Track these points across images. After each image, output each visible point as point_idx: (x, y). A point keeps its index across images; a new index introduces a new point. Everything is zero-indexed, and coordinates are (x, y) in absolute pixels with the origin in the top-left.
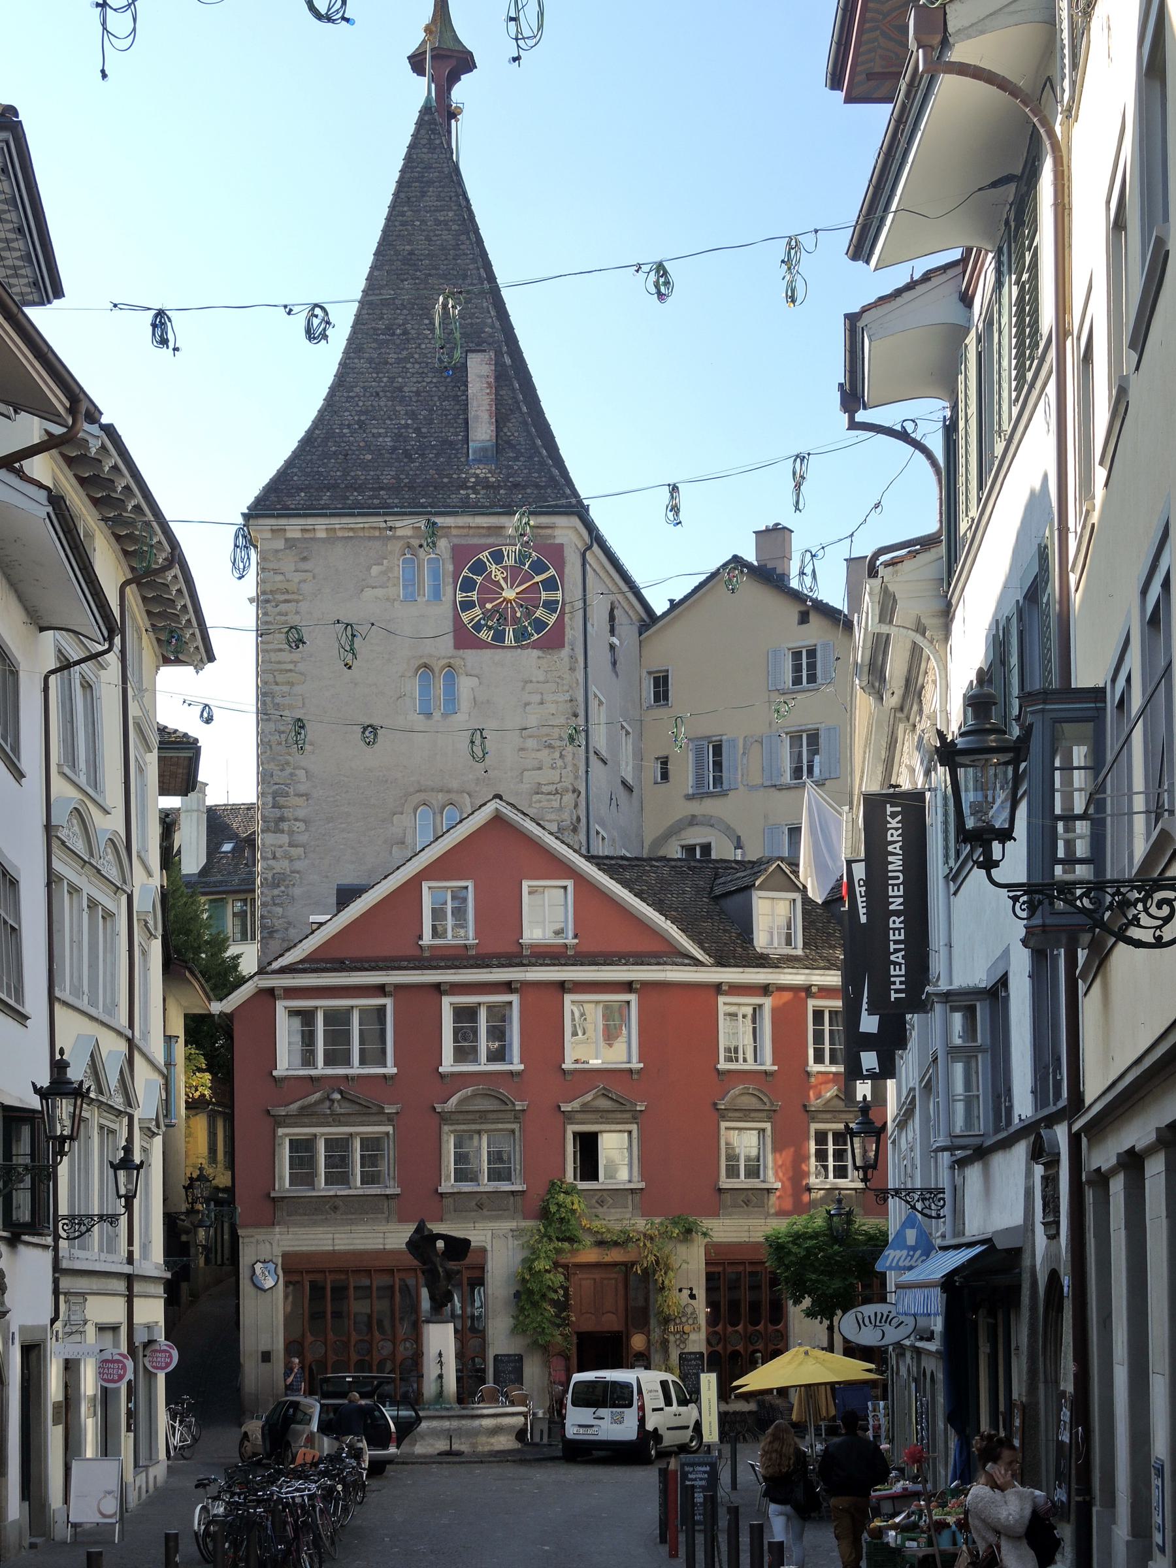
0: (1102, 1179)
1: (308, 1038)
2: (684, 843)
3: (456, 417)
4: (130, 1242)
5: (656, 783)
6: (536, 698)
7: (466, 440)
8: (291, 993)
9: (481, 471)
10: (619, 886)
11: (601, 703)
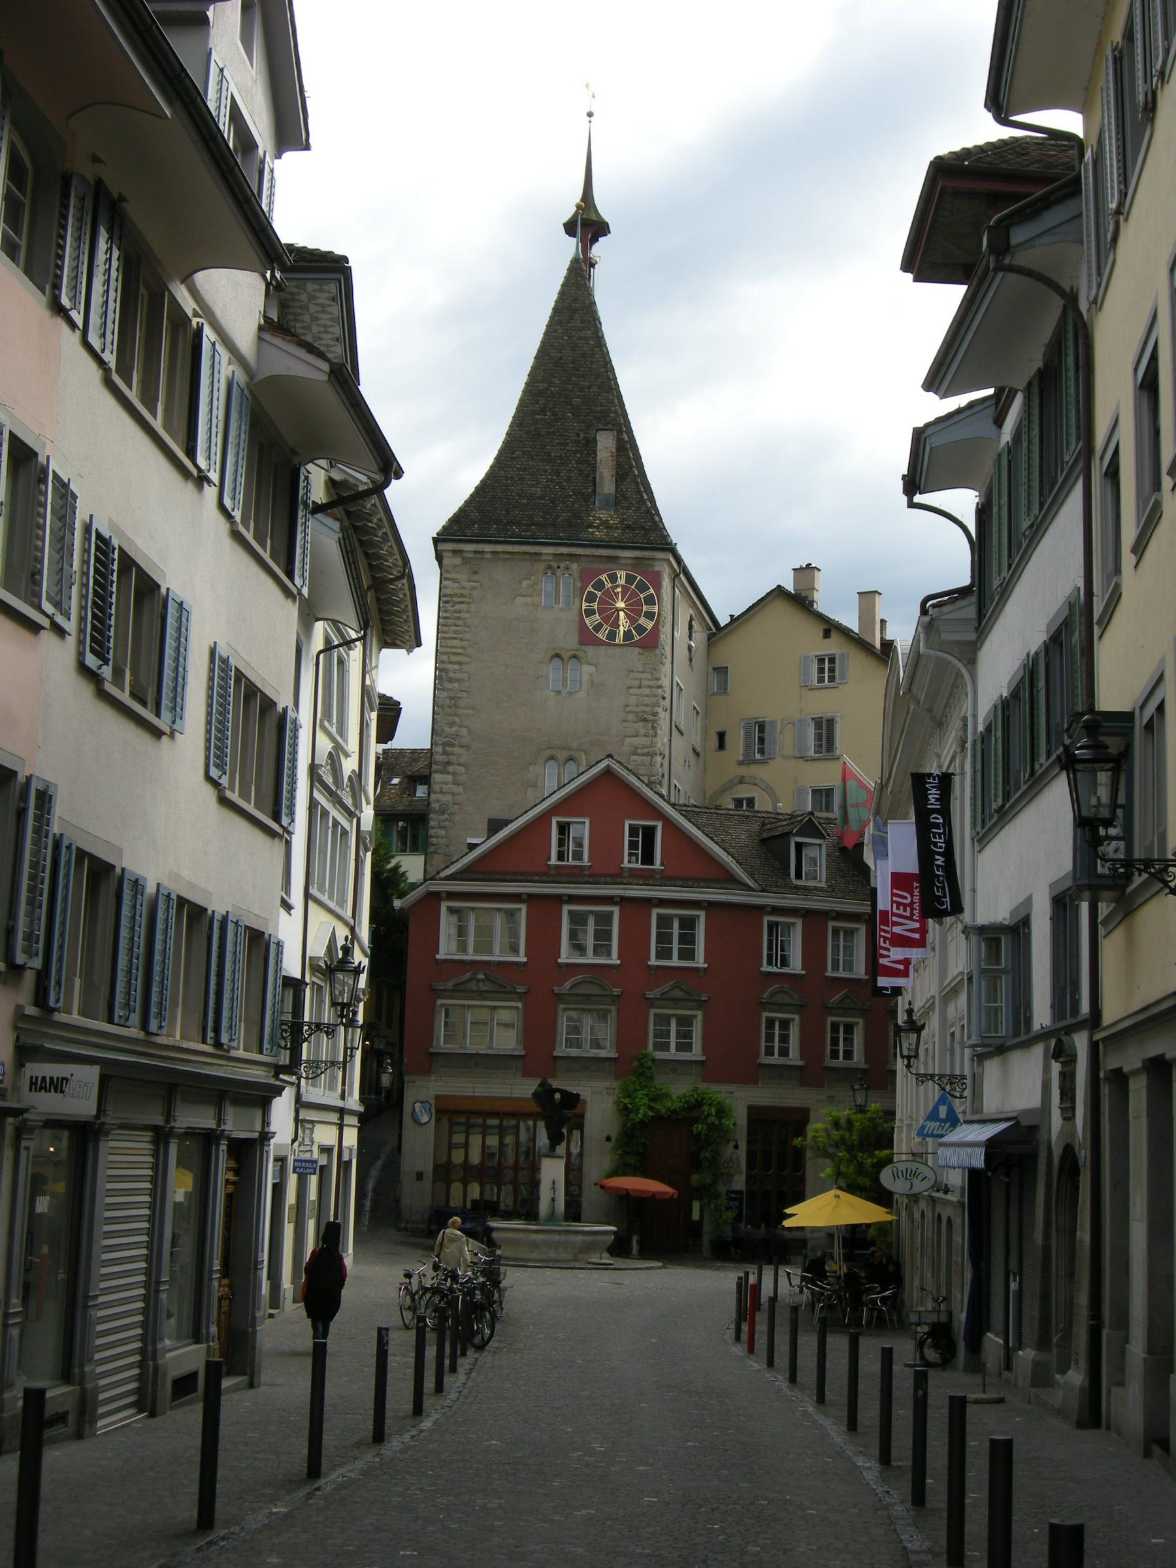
0: (1120, 1078)
3: (588, 475)
4: (344, 1084)
6: (636, 683)
7: (594, 491)
9: (603, 515)
11: (681, 689)
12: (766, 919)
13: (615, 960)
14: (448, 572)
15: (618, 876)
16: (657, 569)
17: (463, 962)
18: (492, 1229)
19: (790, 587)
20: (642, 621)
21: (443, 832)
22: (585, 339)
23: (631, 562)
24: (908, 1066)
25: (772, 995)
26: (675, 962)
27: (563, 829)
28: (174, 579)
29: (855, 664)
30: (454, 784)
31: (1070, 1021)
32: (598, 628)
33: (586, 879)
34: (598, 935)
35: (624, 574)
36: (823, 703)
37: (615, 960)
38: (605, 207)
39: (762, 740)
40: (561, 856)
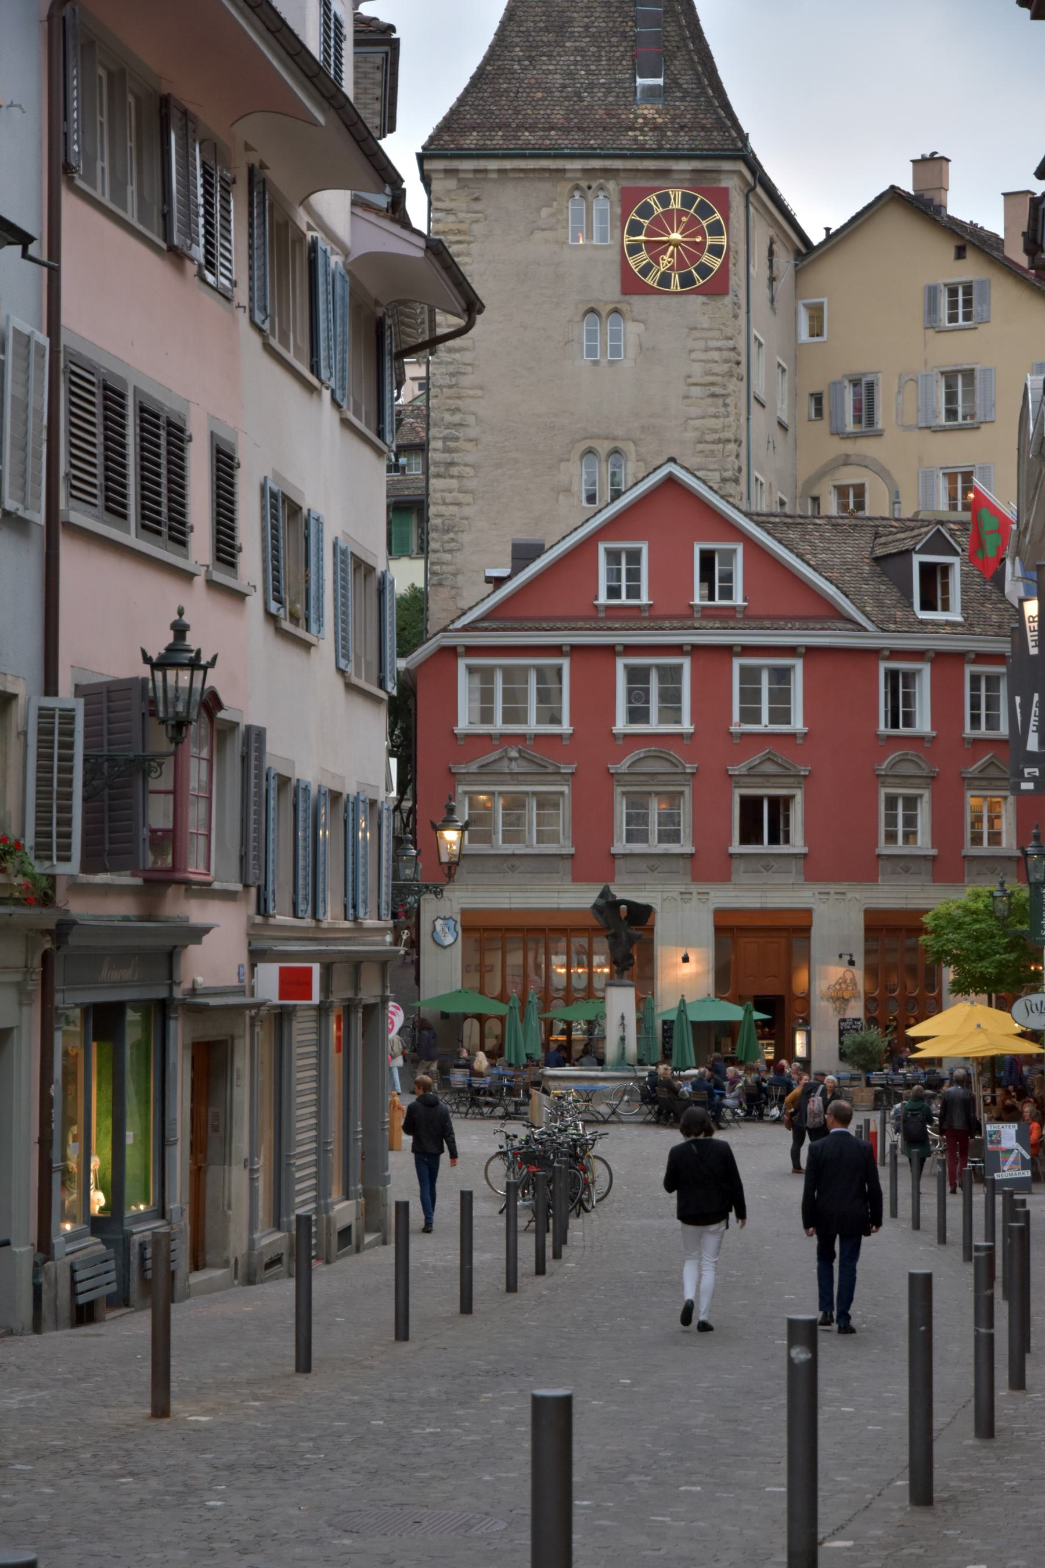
1: (487, 696)
2: (837, 483)
5: (810, 420)
6: (701, 344)
8: (472, 651)
10: (787, 551)
11: (760, 345)
12: (883, 666)
13: (686, 726)
14: (439, 200)
15: (687, 617)
16: (724, 184)
17: (489, 736)
19: (907, 186)
20: (706, 258)
21: (447, 557)
23: (688, 176)
25: (893, 765)
26: (765, 725)
27: (613, 556)
28: (310, 501)
30: (460, 491)
32: (646, 270)
33: (645, 624)
34: (663, 697)
35: (679, 193)
36: (957, 349)
37: (686, 726)
40: (613, 592)
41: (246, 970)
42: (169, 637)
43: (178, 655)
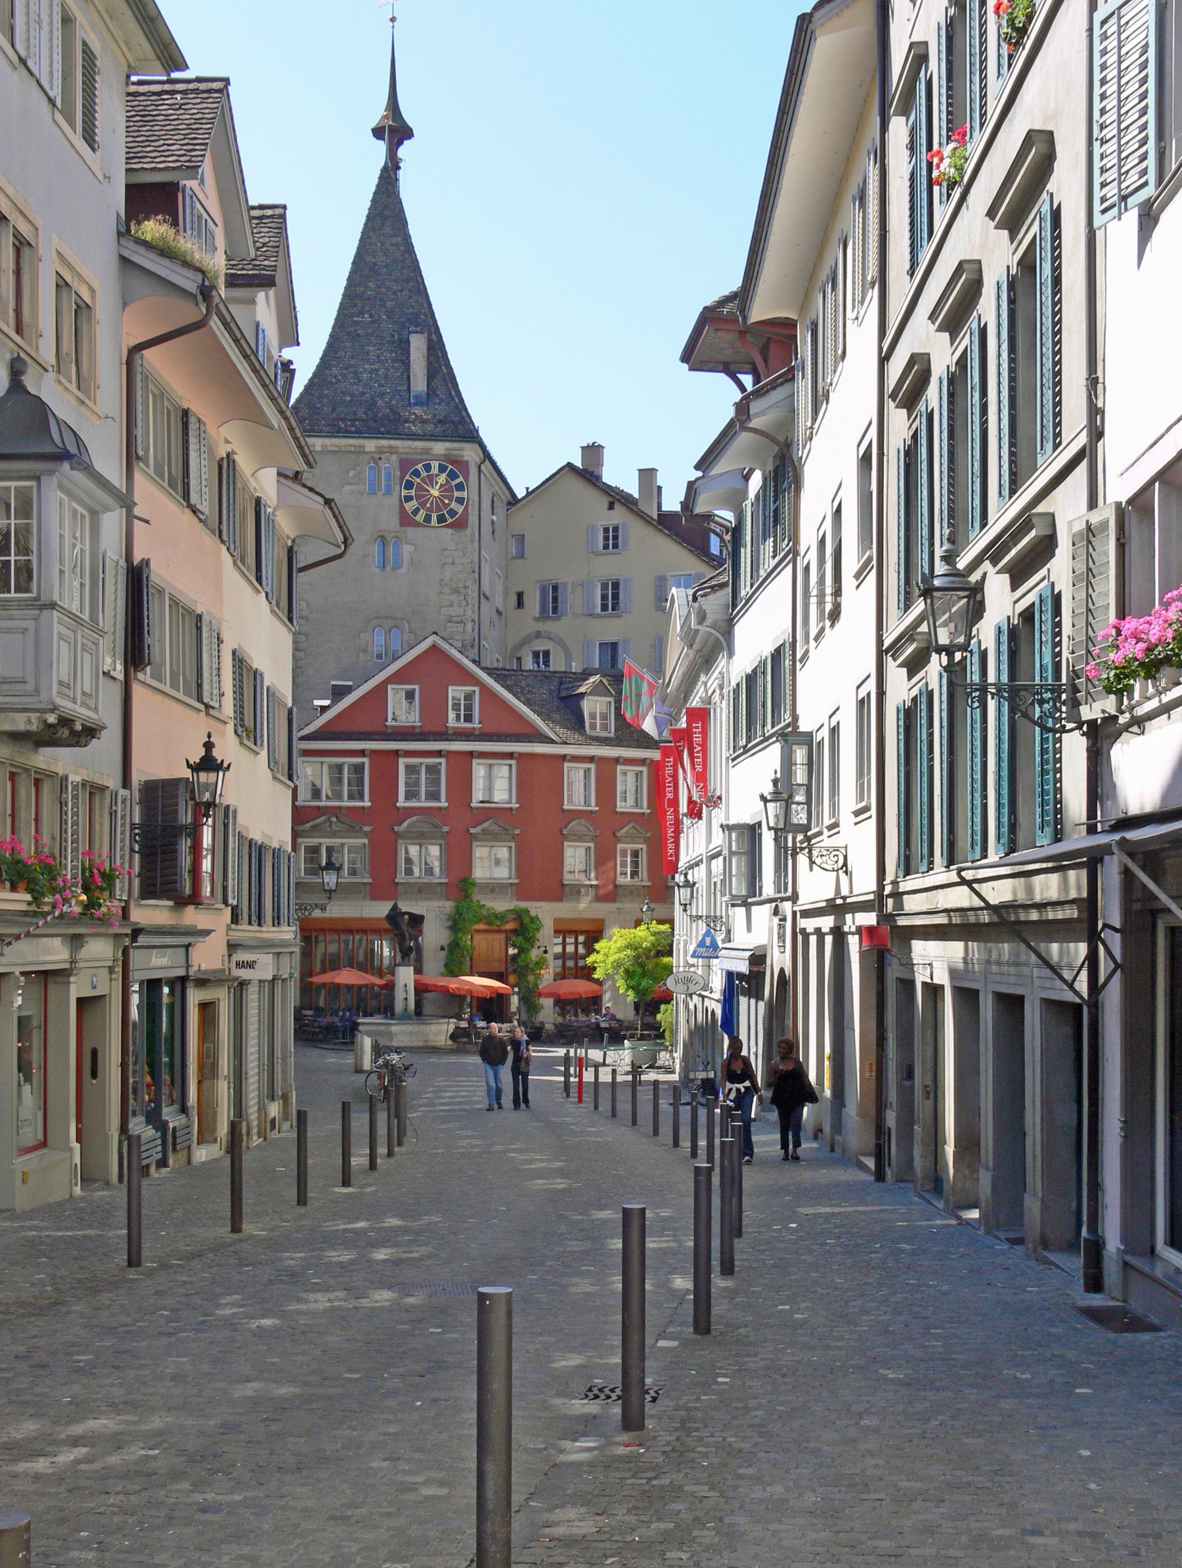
17: (318, 807)
18: (359, 1024)
19: (578, 463)
20: (454, 505)
22: (396, 244)
24: (685, 910)
29: (636, 532)
31: (782, 895)
32: (416, 512)
35: (437, 463)
36: (610, 566)
38: (409, 115)
39: (555, 599)
41: (226, 958)
42: (202, 752)
43: (208, 763)
